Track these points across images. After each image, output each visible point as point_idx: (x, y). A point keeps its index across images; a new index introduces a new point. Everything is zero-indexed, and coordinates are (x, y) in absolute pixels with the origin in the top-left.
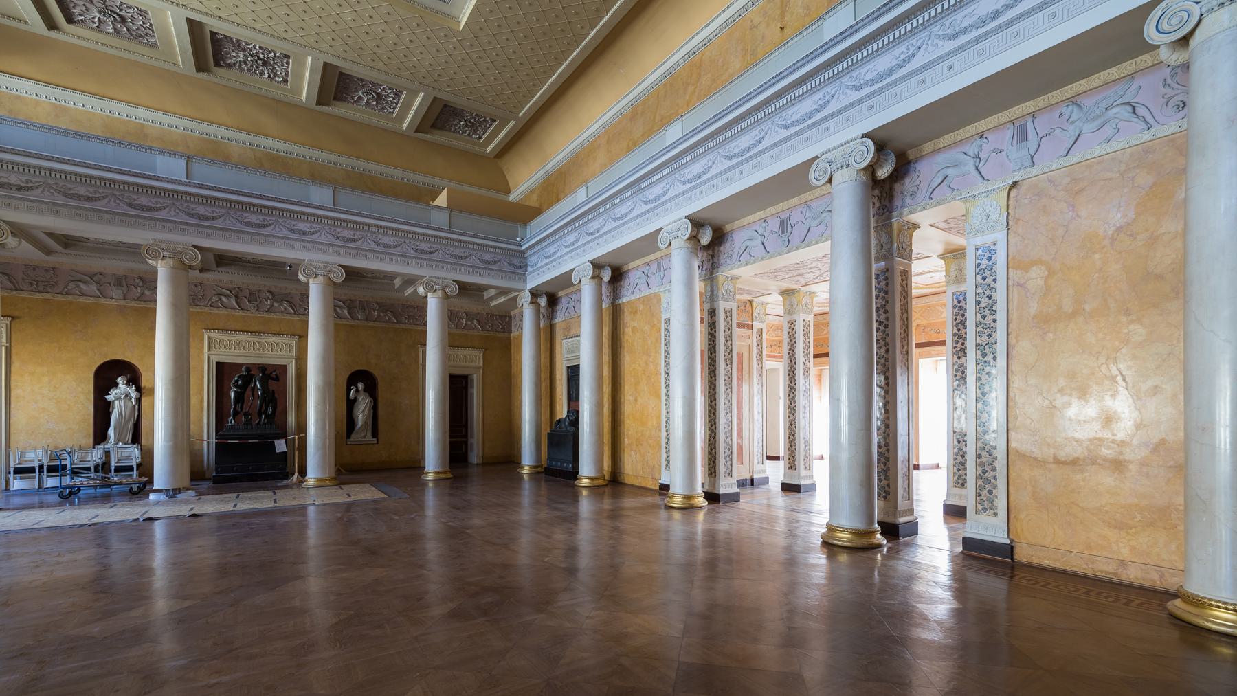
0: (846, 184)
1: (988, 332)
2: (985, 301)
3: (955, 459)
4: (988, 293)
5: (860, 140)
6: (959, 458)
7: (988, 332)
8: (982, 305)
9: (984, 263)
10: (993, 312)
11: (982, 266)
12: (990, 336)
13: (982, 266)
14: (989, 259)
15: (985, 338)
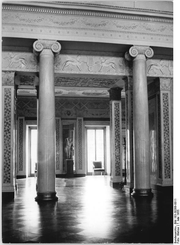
0: (142, 60)
1: (166, 121)
2: (165, 110)
3: (116, 165)
4: (166, 109)
5: (148, 48)
6: (117, 165)
7: (166, 121)
8: (165, 112)
9: (165, 99)
10: (168, 115)
11: (165, 100)
12: (167, 122)
13: (165, 100)
14: (166, 98)
15: (166, 123)
